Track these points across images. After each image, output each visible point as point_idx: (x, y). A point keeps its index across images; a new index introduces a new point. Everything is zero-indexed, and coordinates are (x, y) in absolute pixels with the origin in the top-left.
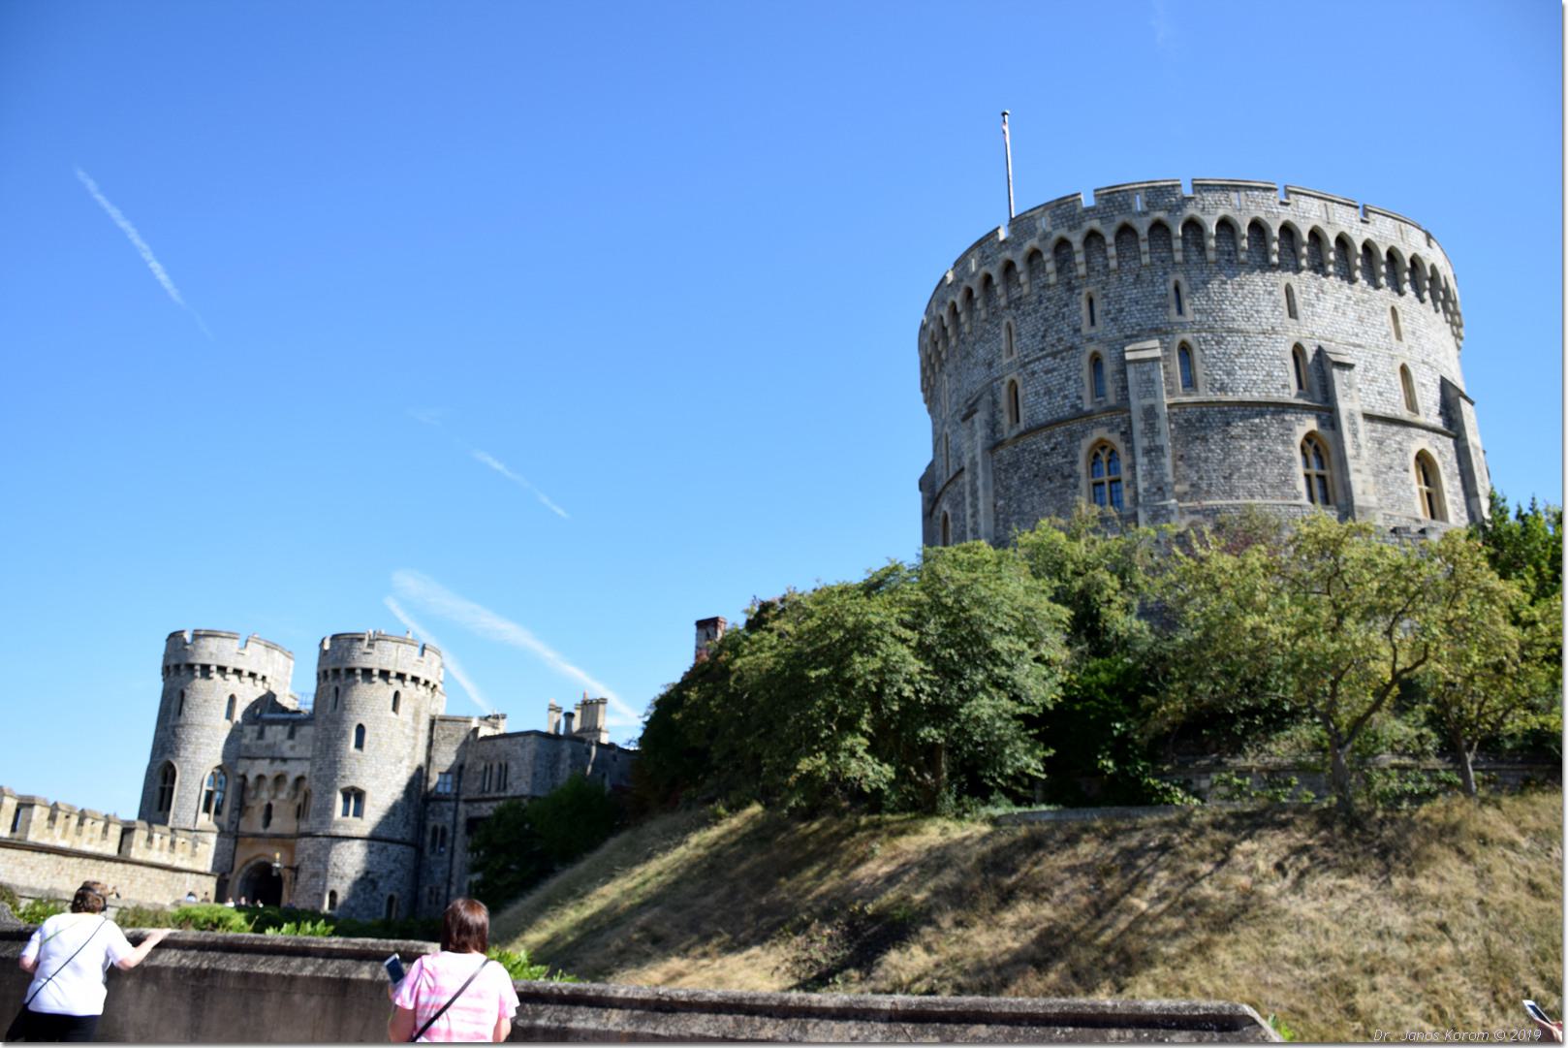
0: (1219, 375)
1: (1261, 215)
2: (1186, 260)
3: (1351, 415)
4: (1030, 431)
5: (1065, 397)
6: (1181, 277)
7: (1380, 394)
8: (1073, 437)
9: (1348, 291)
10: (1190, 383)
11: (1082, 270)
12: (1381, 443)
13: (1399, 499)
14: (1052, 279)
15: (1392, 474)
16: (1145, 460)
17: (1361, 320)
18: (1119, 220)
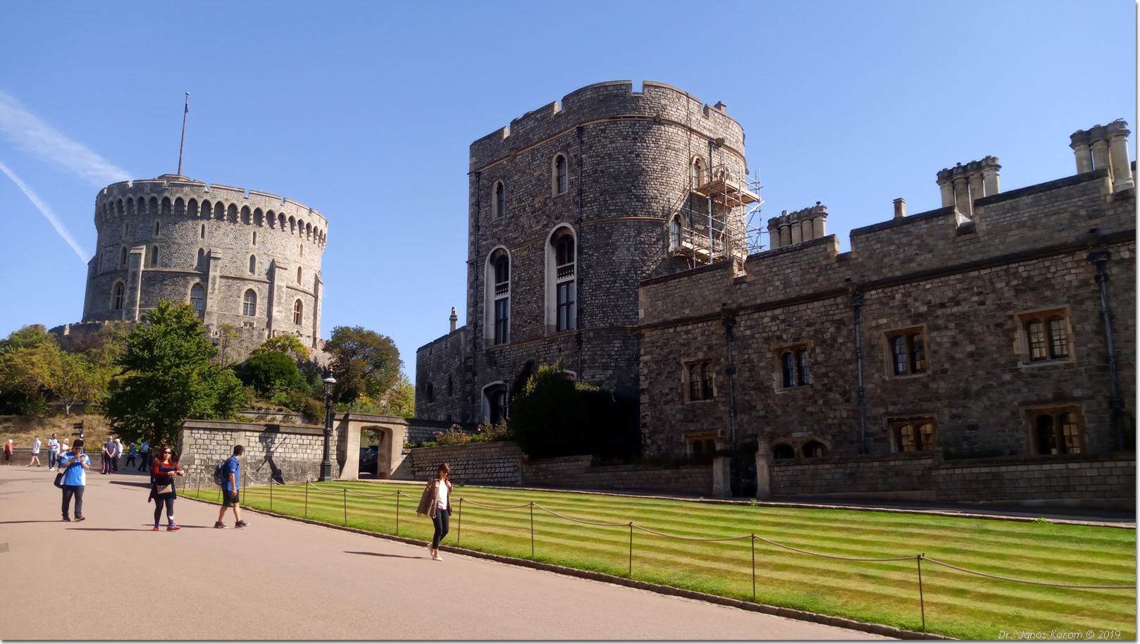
0: (165, 260)
1: (195, 197)
2: (163, 213)
3: (214, 278)
4: (102, 275)
5: (113, 263)
6: (159, 220)
7: (236, 267)
8: (112, 279)
9: (232, 227)
10: (154, 262)
11: (125, 213)
12: (229, 286)
13: (233, 308)
14: (116, 215)
15: (231, 299)
16: (129, 292)
17: (236, 238)
18: (139, 195)
